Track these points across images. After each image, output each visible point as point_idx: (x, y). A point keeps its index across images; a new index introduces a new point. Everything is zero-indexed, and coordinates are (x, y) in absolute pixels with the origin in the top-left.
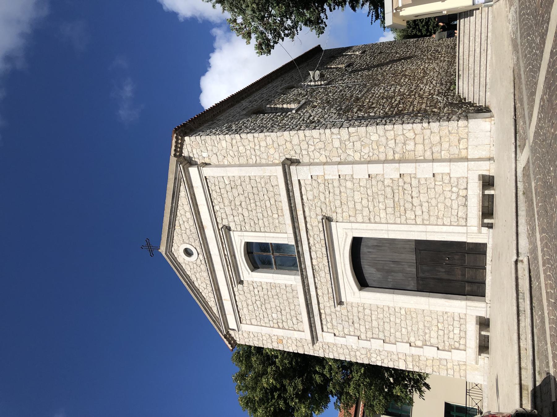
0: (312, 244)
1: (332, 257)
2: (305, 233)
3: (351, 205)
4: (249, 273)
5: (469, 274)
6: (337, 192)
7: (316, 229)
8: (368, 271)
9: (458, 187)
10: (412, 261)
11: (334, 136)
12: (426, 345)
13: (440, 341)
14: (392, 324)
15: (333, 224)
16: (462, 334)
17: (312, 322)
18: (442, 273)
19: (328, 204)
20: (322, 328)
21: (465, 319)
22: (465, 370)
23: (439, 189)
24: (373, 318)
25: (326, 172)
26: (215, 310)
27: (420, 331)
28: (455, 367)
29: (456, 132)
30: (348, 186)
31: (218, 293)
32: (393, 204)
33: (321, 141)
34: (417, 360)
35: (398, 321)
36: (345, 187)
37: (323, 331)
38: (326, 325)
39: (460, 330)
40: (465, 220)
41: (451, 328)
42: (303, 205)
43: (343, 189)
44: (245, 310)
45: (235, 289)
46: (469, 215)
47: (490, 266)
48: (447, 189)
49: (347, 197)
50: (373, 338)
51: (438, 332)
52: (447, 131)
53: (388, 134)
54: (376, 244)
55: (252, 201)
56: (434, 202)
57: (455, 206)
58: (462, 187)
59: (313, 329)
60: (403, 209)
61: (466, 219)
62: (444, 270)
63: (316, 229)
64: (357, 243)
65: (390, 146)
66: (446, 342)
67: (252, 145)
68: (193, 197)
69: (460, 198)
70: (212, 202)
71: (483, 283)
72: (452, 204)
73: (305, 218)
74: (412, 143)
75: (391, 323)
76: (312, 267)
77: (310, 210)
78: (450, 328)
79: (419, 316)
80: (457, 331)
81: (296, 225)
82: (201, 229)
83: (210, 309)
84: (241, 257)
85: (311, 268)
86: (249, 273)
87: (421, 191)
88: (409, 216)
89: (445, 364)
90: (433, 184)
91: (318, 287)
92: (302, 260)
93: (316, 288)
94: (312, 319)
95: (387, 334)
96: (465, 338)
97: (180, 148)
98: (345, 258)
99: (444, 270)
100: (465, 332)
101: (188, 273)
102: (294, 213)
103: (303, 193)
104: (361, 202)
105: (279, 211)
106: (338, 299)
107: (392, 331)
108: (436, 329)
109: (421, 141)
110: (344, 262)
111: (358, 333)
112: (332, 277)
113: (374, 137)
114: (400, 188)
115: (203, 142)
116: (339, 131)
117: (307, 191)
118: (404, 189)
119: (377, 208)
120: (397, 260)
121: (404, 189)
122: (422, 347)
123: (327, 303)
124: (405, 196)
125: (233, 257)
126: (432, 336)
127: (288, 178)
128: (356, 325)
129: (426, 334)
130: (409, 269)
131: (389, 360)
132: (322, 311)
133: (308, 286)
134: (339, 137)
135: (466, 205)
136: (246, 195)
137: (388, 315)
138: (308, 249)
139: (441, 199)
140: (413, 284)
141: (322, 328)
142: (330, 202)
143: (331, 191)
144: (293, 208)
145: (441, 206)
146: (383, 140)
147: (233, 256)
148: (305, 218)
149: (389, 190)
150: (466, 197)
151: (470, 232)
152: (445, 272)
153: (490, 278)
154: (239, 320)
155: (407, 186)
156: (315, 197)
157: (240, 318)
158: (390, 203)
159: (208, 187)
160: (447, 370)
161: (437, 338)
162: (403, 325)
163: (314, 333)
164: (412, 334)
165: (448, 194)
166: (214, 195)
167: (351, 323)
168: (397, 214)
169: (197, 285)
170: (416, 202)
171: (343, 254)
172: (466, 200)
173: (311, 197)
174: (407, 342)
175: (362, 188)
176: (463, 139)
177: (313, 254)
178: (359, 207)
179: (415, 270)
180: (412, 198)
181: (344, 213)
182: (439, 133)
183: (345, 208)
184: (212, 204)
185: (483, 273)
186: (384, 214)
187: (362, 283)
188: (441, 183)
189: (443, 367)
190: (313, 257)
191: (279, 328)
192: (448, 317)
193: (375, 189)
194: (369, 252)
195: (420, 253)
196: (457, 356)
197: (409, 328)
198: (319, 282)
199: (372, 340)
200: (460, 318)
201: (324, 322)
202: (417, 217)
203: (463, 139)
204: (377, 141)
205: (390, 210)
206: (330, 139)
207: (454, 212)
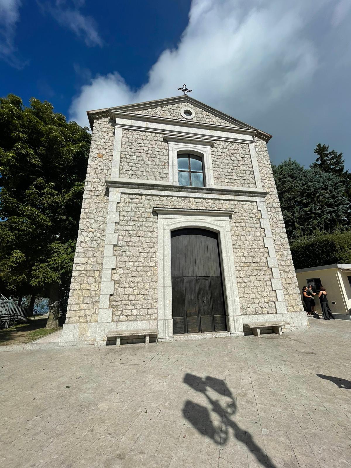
0: (207, 201)
1: (168, 212)
2: (218, 198)
3: (244, 233)
4: (176, 149)
5: (193, 319)
6: (251, 225)
7: (221, 206)
8: (185, 239)
9: (268, 307)
10: (198, 273)
11: (281, 229)
12: (115, 284)
13: (121, 296)
14: (137, 254)
15: (228, 219)
16: (133, 317)
17: (134, 186)
18: (189, 297)
19: (241, 217)
20: (125, 193)
21: (151, 319)
22: (79, 322)
23: (264, 294)
24: (141, 238)
25: (265, 220)
26: (141, 112)
27: (132, 279)
28: (83, 312)
29: (297, 304)
30: (256, 233)
31: (154, 120)
32: (249, 262)
33: (277, 220)
34: (88, 275)
35: (141, 259)
36: (256, 231)
37: (122, 193)
38: (128, 197)
39: (137, 315)
40: (245, 313)
41: (139, 306)
42: (238, 201)
43: (254, 229)
44: (138, 136)
45: (161, 135)
46: (251, 317)
47: (211, 337)
48: (265, 299)
49: (249, 232)
50: (118, 235)
51: (133, 294)
52: (297, 298)
53: (288, 261)
54: (209, 247)
55: (235, 168)
56: (255, 290)
57: (255, 306)
58: (269, 310)
59: (125, 186)
60: (246, 269)
61: (246, 315)
62: (193, 298)
63: (221, 206)
64: (214, 235)
65: (282, 262)
66: (120, 303)
67: (268, 179)
68: (234, 131)
69: (261, 309)
70: (230, 142)
71: (186, 331)
72: (255, 303)
73: (228, 200)
74: (286, 276)
75: (138, 253)
76: (187, 197)
77: (235, 205)
78: (138, 306)
79: (149, 278)
80: (135, 312)
81: (225, 193)
82: (221, 129)
83: (137, 110)
84: (190, 148)
85: (187, 196)
86: (176, 149)
87: (261, 282)
88: (242, 273)
89: (85, 302)
90: (267, 290)
91: (168, 199)
92: (195, 190)
93: (167, 196)
94: (137, 186)
95: (124, 249)
96: (128, 320)
97: (261, 135)
98: (201, 223)
99: (193, 298)
100: (136, 320)
101: (169, 107)
102: (234, 193)
103: (247, 203)
104: (246, 240)
105: (231, 184)
106: (161, 212)
107: (129, 254)
108: (136, 293)
109: (288, 282)
110: (197, 221)
111: (122, 223)
112: (185, 210)
113: (285, 253)
114: (261, 268)
115: (264, 151)
116: (284, 232)
117: (249, 205)
118: (260, 270)
119: (244, 251)
120: (197, 262)
121: (260, 270)
122: (112, 280)
123: (155, 202)
124: (256, 271)
125: (189, 142)
126: (126, 289)
127: (258, 195)
128: (132, 223)
129: (129, 284)
130: (190, 271)
131: (86, 249)
132: (144, 197)
133: (171, 191)
134: (282, 232)
135: (256, 313)
136: (239, 165)
137: (147, 251)
138: (204, 197)
139: (259, 296)
140: (177, 274)
141: (125, 193)
142: (243, 219)
143: (251, 221)
144: (237, 193)
145: (253, 296)
146: (285, 259)
147: (191, 142)
148: (228, 200)
149: (259, 260)
150: (262, 313)
151: (237, 320)
152: (191, 299)
153: (200, 338)
154: (126, 128)
155: (263, 272)
156: (245, 210)
157: (129, 130)
158: (250, 260)
159: (241, 143)
160: (78, 304)
161: (125, 294)
162: (136, 263)
163: (120, 185)
164: (127, 271)
165: (262, 300)
166: (236, 145)
167: (133, 218)
168: (242, 264)
169: (158, 108)
170: (253, 278)
171: (205, 222)
172: (260, 314)
173: (244, 207)
174: (116, 266)
175: (257, 242)
176: (294, 308)
177: (200, 200)
178: (243, 238)
179: (190, 276)
180: (255, 275)
181: (236, 228)
182: (295, 293)
183: (241, 229)
184: (229, 142)
185: (195, 330)
186: (240, 255)
187: (175, 233)
188: (269, 295)
189: (81, 300)
190: (197, 199)
191: (121, 158)
192: (151, 304)
193: (257, 250)
194: (201, 242)
195: (206, 280)
196: (105, 314)
197: (134, 269)
198: (174, 200)
199: (117, 234)
200: (151, 315)
201: (131, 196)
202: (241, 278)
203: (294, 308)
204: (283, 254)
205: (244, 259)
206: (279, 226)
207: (250, 305)
